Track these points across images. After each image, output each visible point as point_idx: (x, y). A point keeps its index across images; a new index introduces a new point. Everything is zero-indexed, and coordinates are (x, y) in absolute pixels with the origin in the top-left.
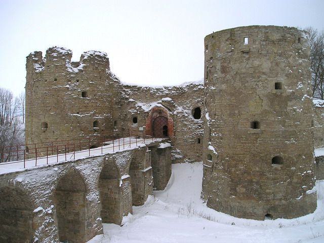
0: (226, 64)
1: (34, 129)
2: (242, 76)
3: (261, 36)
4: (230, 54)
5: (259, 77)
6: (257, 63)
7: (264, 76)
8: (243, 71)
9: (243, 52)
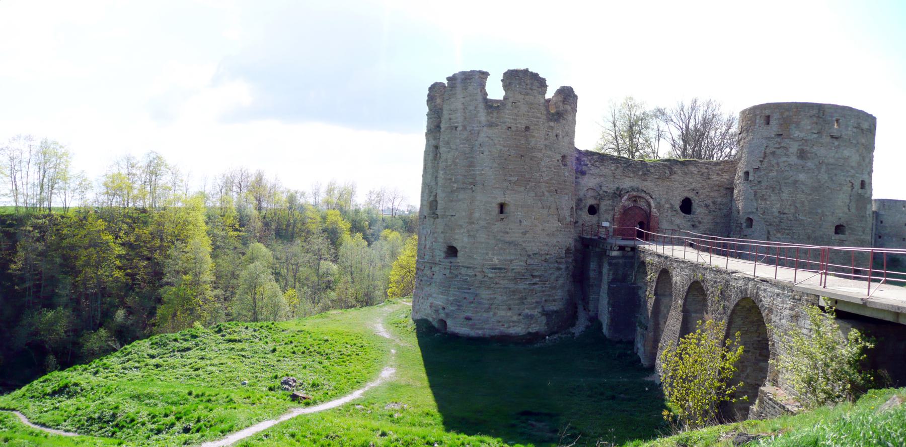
0: (808, 148)
1: (477, 215)
2: (831, 167)
3: (852, 122)
4: (815, 136)
5: (848, 171)
6: (846, 153)
7: (853, 171)
8: (832, 161)
9: (832, 137)
